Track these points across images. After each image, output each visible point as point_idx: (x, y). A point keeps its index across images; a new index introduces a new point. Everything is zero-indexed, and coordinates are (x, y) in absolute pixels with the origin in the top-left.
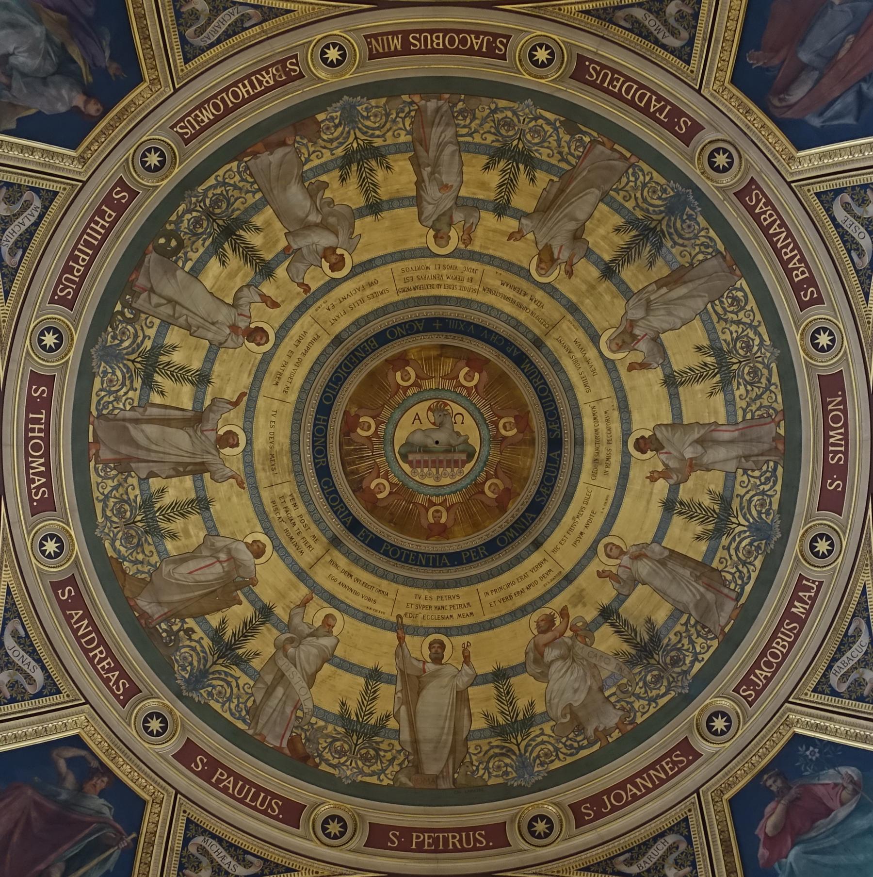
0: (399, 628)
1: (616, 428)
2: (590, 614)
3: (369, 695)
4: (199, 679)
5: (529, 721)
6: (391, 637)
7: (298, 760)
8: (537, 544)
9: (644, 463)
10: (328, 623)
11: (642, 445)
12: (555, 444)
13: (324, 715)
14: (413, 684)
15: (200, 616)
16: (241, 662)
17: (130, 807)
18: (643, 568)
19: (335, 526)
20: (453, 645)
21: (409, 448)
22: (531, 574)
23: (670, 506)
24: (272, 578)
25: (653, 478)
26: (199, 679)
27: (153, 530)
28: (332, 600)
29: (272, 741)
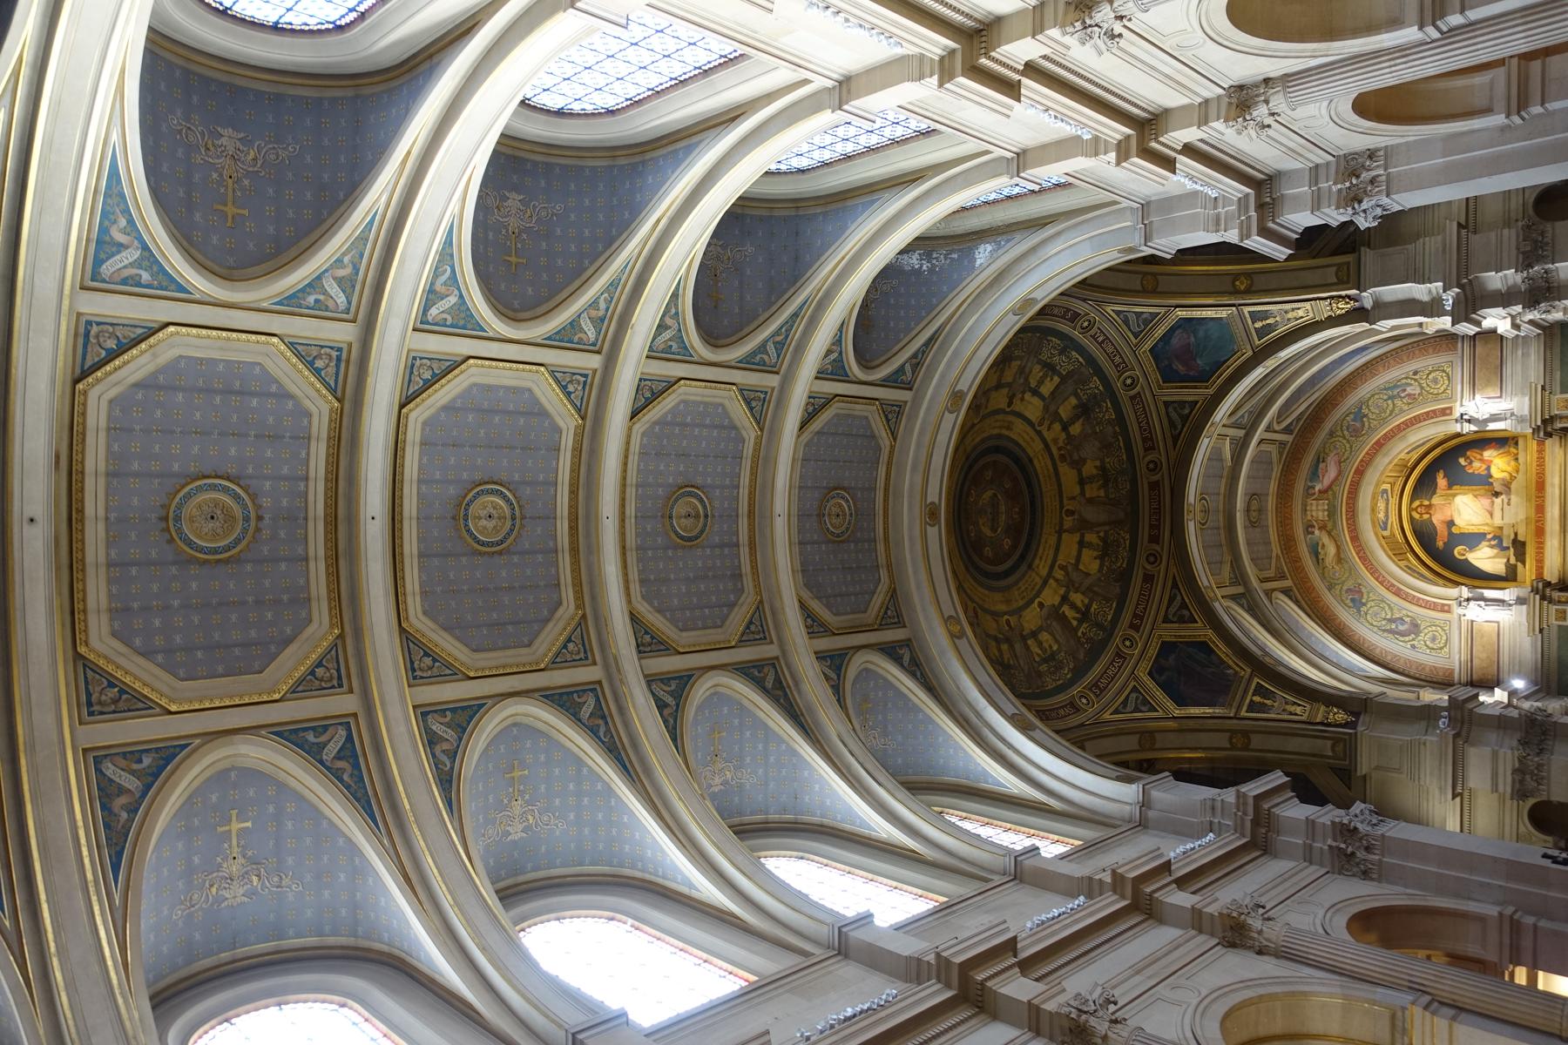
0: (1060, 532)
1: (1000, 417)
2: (1063, 435)
3: (1090, 546)
4: (1100, 626)
5: (1103, 468)
6: (1064, 536)
7: (1124, 577)
8: (1031, 460)
9: (1018, 406)
10: (1062, 568)
11: (1010, 404)
12: (997, 449)
13: (1101, 566)
14: (1084, 525)
15: (1076, 630)
16: (1088, 607)
17: (1167, 648)
18: (1052, 408)
19: (1024, 567)
20: (1068, 505)
21: (994, 530)
22: (1041, 464)
23: (1035, 392)
24: (1050, 597)
25: (1022, 399)
26: (1100, 626)
27: (1053, 656)
28: (1052, 567)
29: (1118, 590)
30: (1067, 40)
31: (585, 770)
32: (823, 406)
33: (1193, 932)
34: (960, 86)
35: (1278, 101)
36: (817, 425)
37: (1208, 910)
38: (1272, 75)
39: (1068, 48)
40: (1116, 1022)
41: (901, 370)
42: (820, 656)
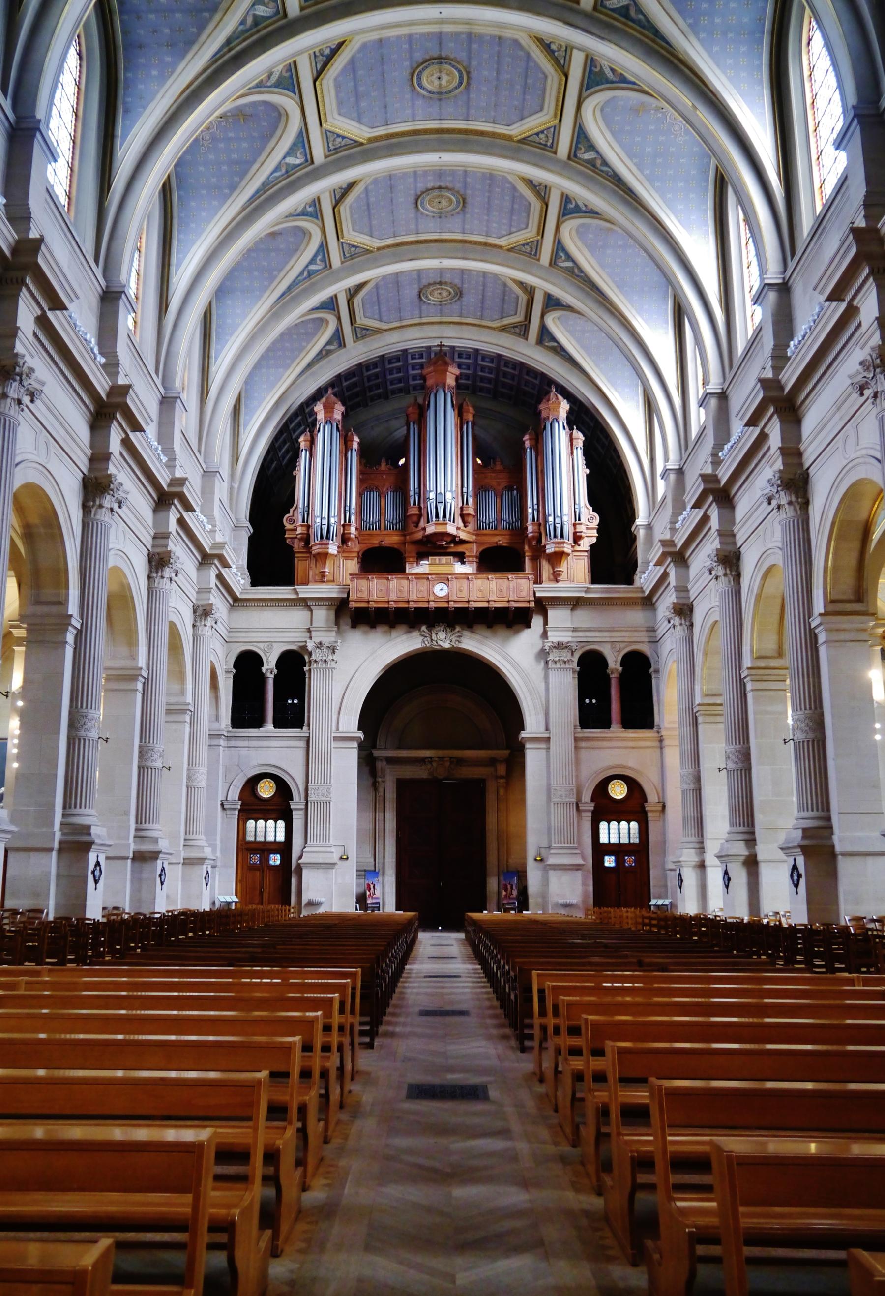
30: (867, 350)
31: (206, 14)
32: (556, 61)
33: (152, 534)
34: (699, 486)
35: (789, 512)
36: (538, 55)
37: (170, 543)
38: (810, 507)
39: (862, 348)
40: (171, 580)
41: (553, 339)
42: (316, 202)
